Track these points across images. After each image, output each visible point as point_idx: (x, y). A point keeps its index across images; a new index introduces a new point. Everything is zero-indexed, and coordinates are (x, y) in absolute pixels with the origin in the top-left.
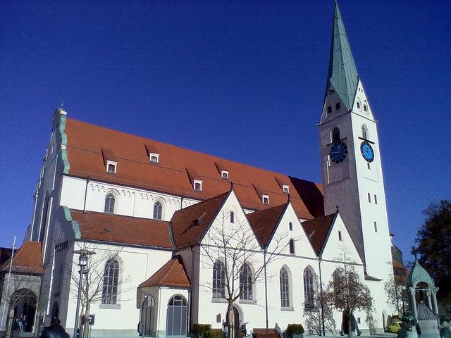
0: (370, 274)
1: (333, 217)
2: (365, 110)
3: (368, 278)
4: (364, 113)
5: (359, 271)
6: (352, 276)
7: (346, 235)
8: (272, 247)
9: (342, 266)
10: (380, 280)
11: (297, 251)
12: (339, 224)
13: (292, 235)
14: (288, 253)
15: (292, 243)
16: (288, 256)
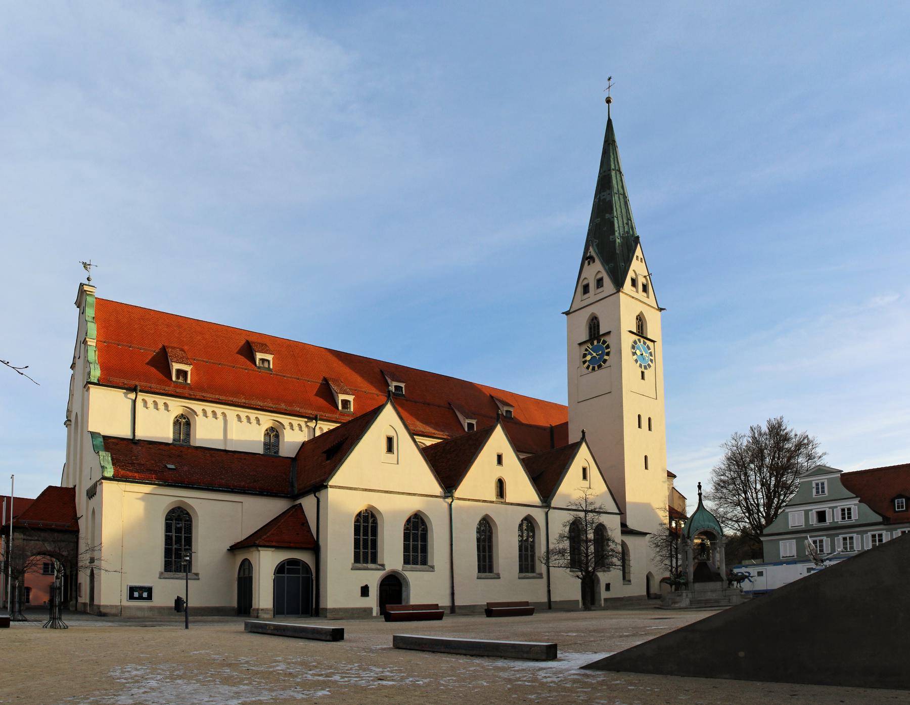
0: (631, 524)
1: (576, 447)
2: (645, 288)
3: (626, 530)
4: (641, 295)
5: (612, 524)
6: (600, 529)
7: (594, 472)
8: (464, 489)
9: (582, 514)
10: (645, 534)
11: (510, 497)
12: (583, 457)
13: (499, 472)
14: (493, 498)
15: (501, 484)
16: (492, 502)
